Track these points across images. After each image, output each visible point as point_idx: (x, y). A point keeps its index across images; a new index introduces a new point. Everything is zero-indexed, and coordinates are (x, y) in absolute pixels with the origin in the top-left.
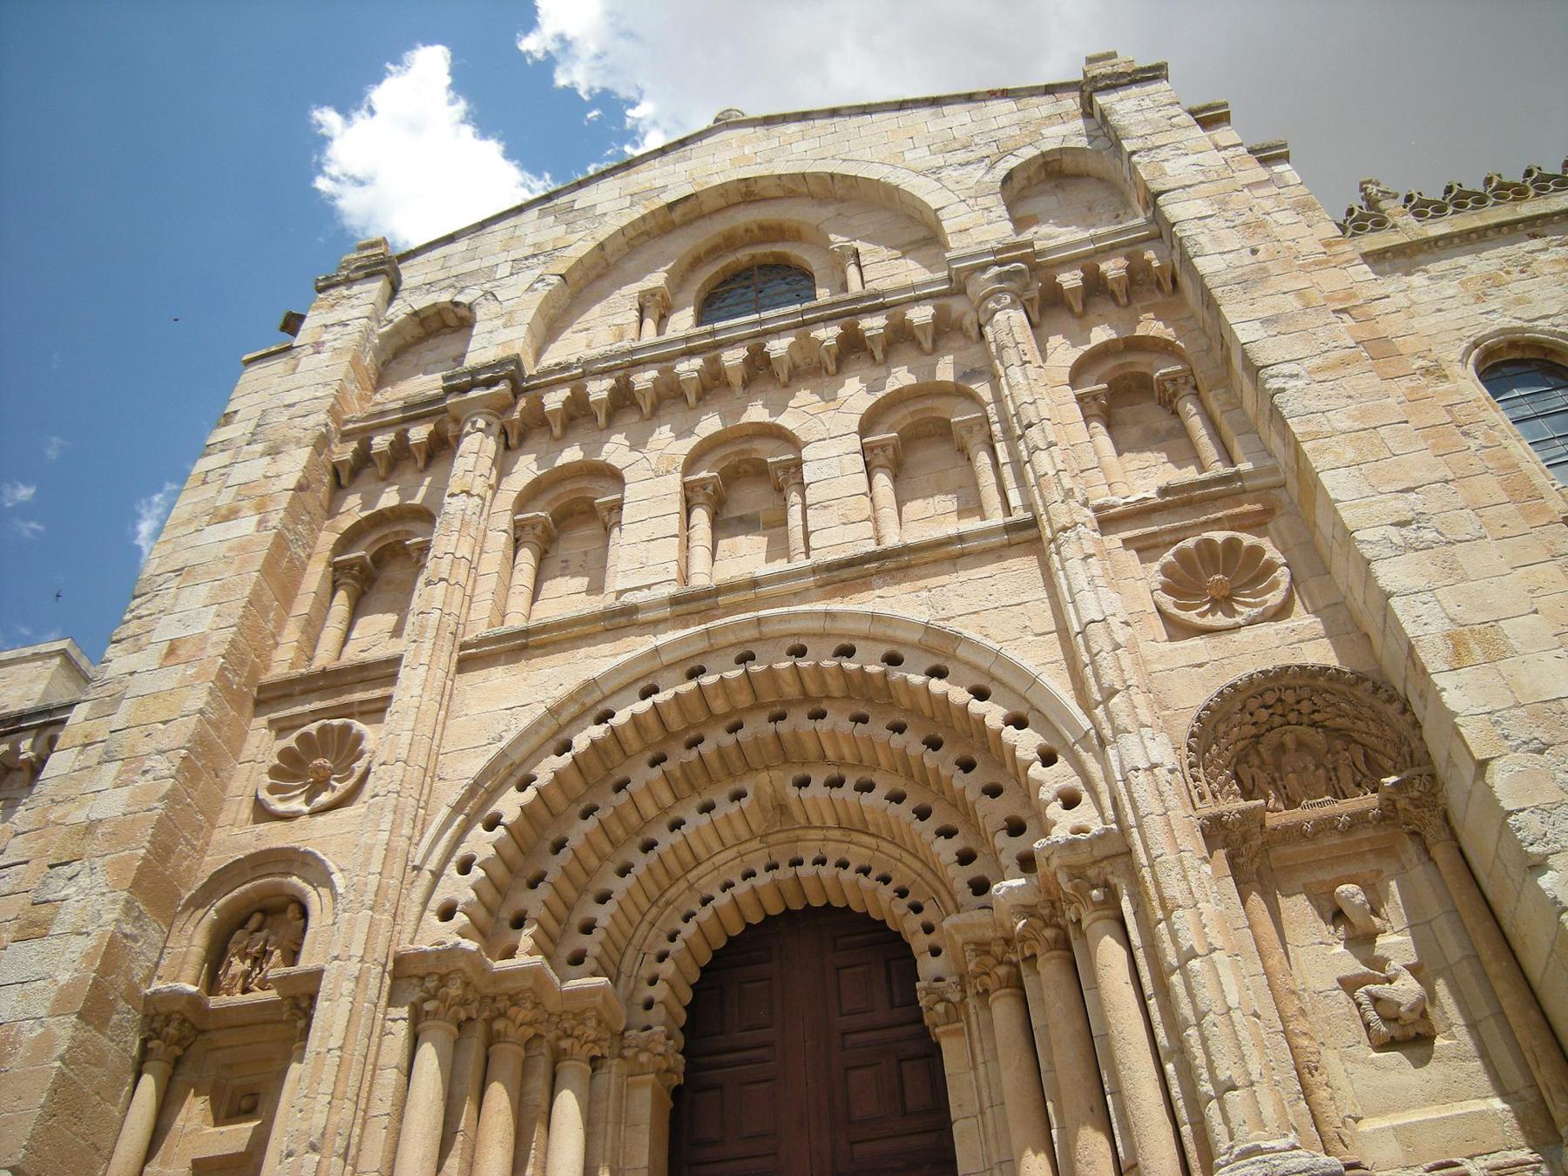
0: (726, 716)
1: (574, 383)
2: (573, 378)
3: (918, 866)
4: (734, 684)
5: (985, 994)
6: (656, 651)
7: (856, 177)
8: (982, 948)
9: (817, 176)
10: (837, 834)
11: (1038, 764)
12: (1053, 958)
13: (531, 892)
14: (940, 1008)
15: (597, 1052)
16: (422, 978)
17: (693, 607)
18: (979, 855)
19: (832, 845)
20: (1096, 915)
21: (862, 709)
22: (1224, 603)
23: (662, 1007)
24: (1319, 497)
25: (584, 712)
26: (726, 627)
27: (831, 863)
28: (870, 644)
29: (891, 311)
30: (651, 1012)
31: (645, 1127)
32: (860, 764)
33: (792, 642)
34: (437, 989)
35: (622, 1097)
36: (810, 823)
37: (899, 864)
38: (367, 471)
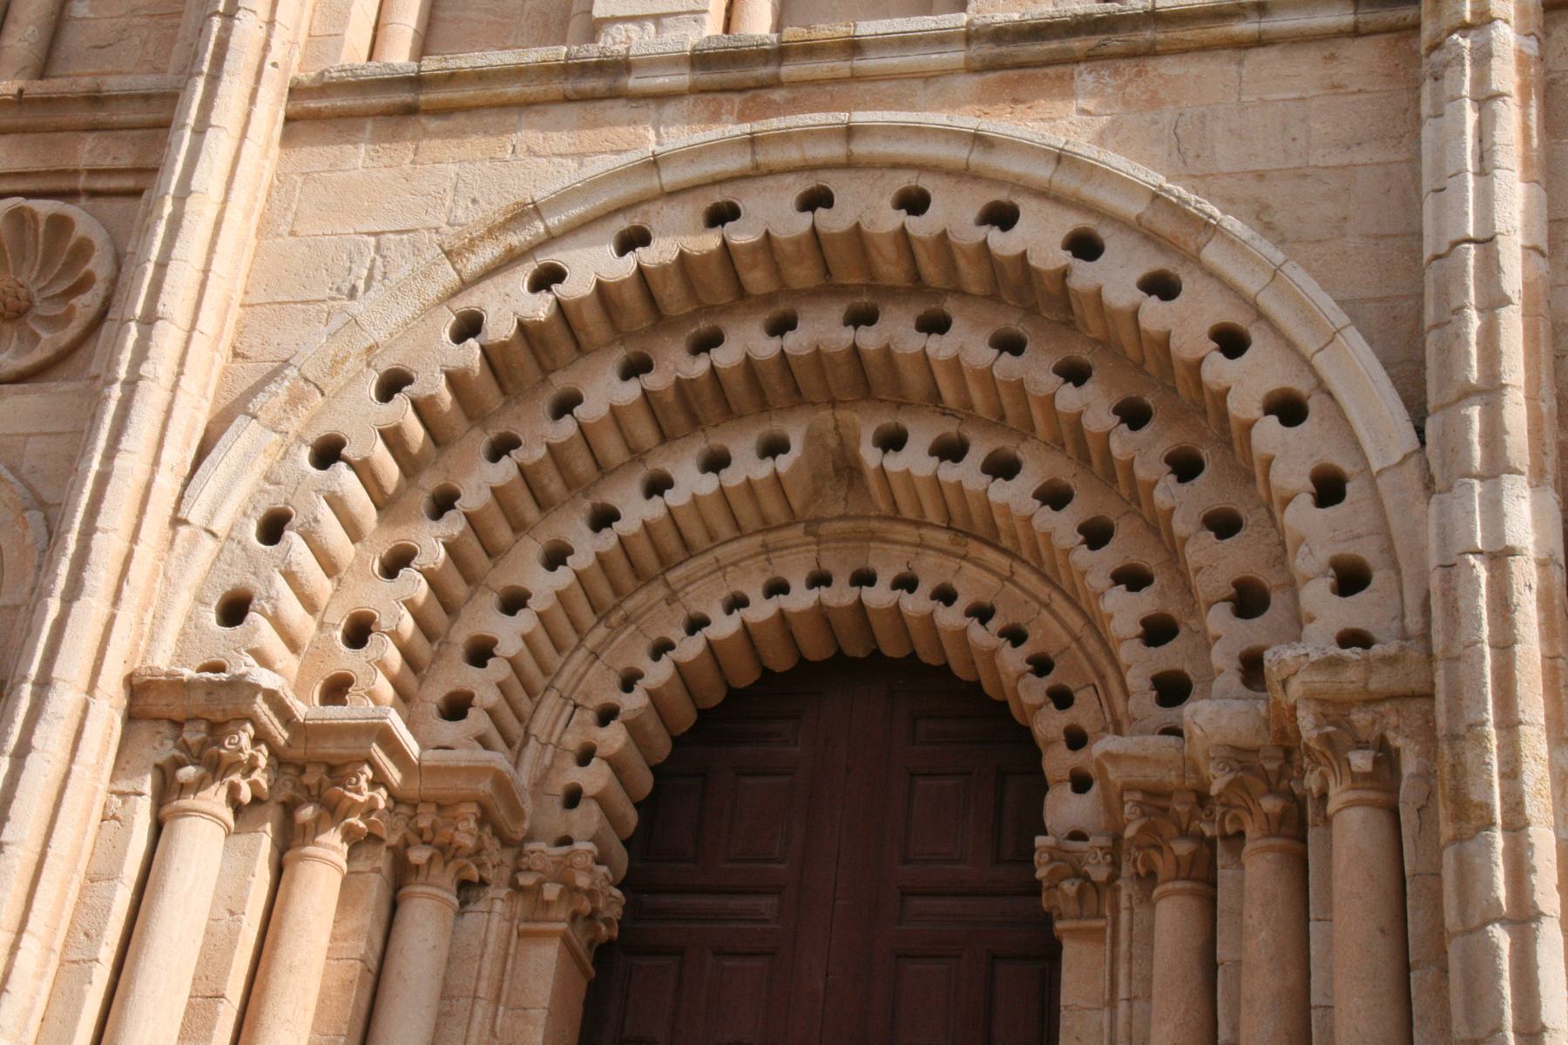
0: (768, 299)
3: (1076, 622)
4: (789, 249)
5: (1148, 879)
6: (654, 164)
8: (1155, 798)
10: (942, 538)
11: (1305, 500)
12: (1271, 849)
13: (386, 584)
14: (1069, 887)
15: (474, 873)
16: (178, 725)
17: (733, 75)
18: (1183, 630)
19: (931, 559)
20: (1352, 795)
23: (594, 807)
25: (512, 259)
26: (786, 137)
27: (925, 588)
28: (1048, 209)
30: (575, 814)
31: (540, 1015)
33: (904, 180)
34: (204, 745)
35: (506, 955)
36: (898, 511)
37: (1045, 613)
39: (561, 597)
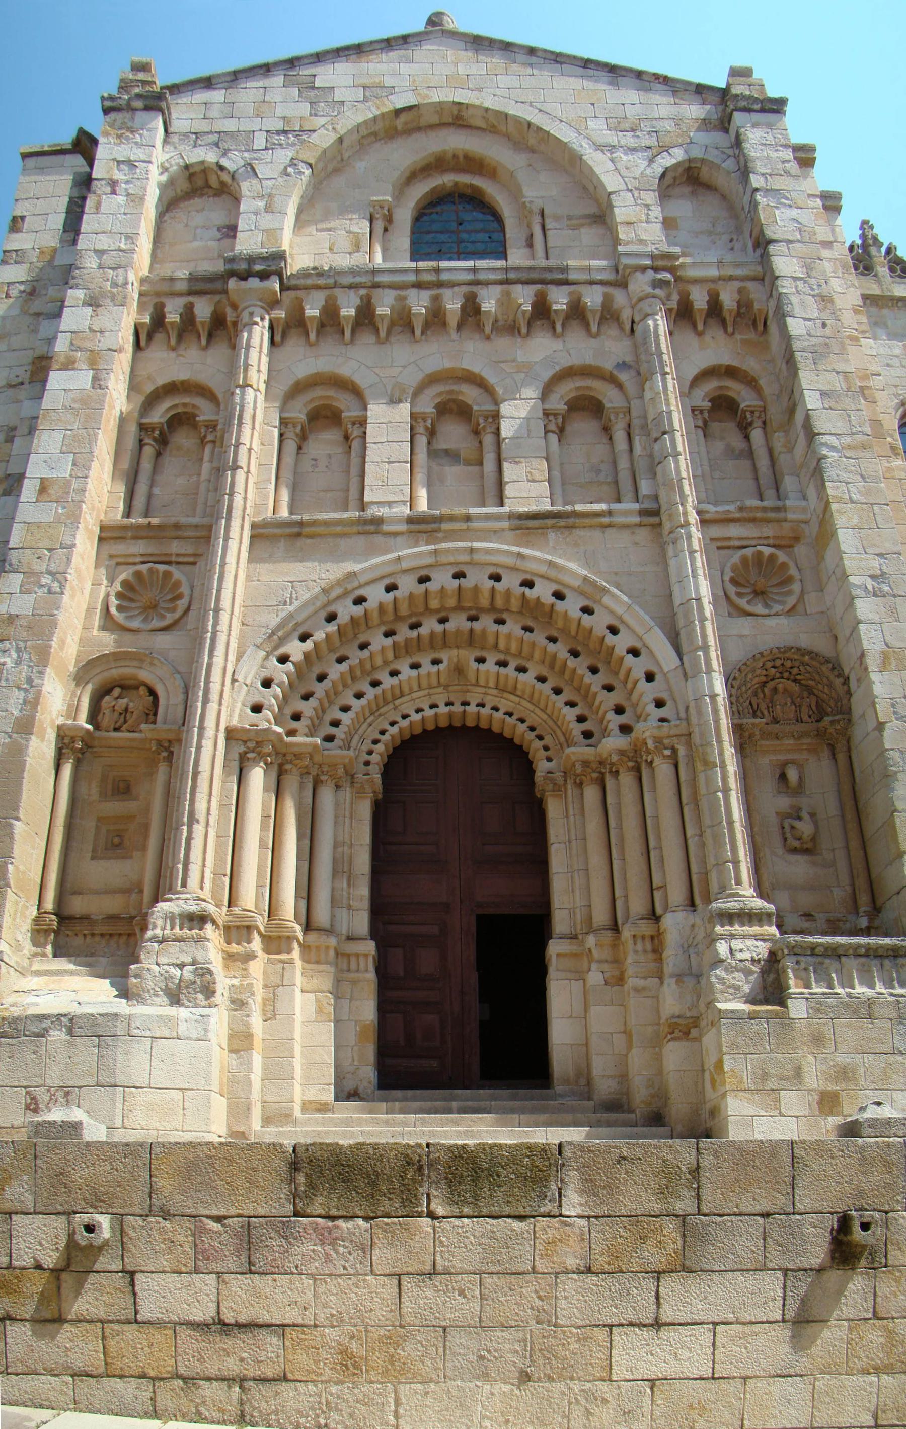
1: (327, 292)
2: (326, 287)
3: (545, 717)
7: (548, 133)
9: (517, 121)
21: (530, 623)
22: (759, 594)
24: (832, 545)
26: (448, 550)
28: (546, 582)
29: (572, 288)
32: (519, 655)
33: (492, 570)
38: (159, 337)
39: (363, 707)
